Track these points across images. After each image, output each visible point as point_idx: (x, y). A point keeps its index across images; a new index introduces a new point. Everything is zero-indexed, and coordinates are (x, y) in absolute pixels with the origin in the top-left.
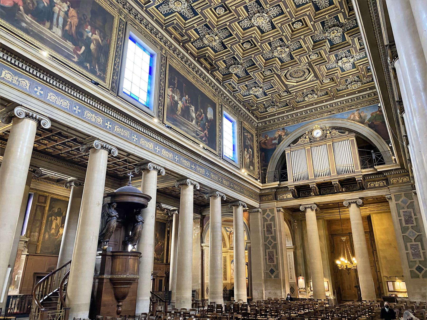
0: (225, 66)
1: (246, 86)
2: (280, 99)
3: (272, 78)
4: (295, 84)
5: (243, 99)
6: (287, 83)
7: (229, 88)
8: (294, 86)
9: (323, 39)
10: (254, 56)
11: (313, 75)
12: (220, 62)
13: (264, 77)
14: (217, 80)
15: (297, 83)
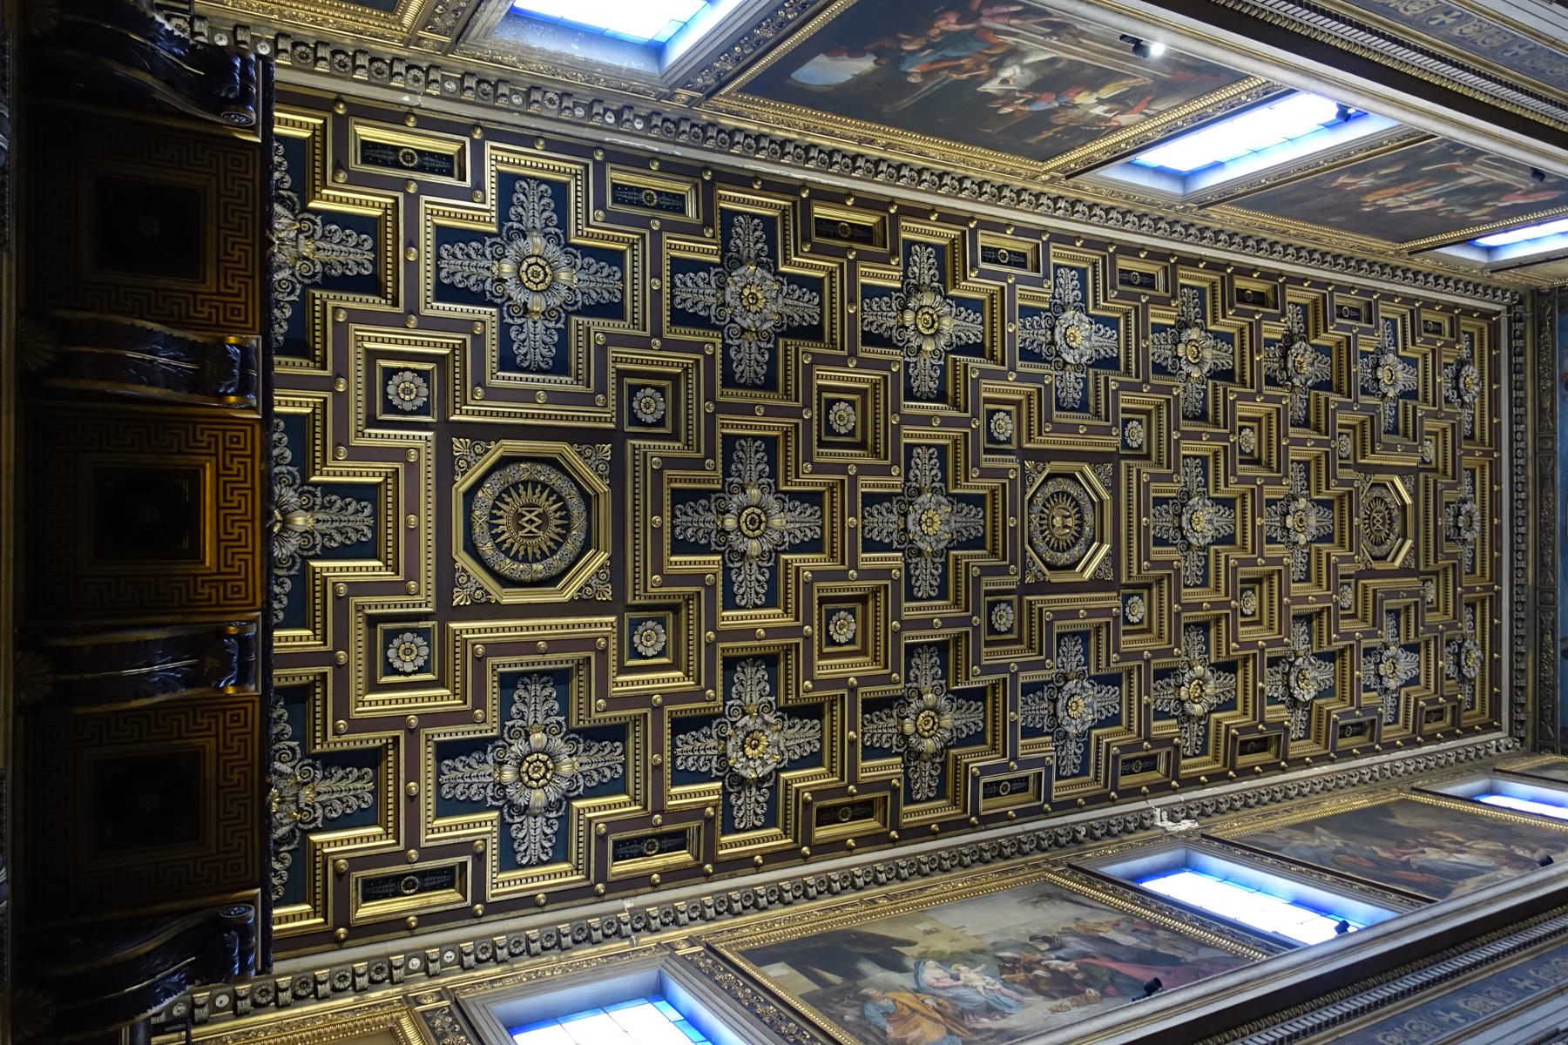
0: (899, 759)
1: (1029, 732)
2: (1160, 637)
3: (1036, 612)
4: (1106, 548)
5: (1096, 780)
6: (1087, 575)
7: (1008, 803)
8: (1114, 555)
9: (943, 369)
10: (901, 622)
11: (1087, 469)
12: (864, 770)
13: (1019, 641)
14: (948, 827)
15: (1102, 542)
